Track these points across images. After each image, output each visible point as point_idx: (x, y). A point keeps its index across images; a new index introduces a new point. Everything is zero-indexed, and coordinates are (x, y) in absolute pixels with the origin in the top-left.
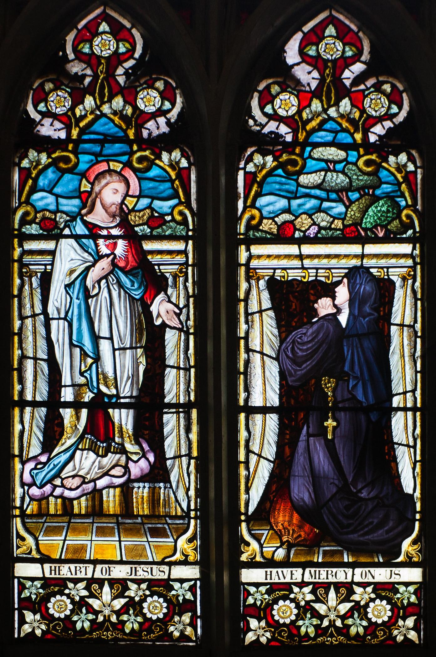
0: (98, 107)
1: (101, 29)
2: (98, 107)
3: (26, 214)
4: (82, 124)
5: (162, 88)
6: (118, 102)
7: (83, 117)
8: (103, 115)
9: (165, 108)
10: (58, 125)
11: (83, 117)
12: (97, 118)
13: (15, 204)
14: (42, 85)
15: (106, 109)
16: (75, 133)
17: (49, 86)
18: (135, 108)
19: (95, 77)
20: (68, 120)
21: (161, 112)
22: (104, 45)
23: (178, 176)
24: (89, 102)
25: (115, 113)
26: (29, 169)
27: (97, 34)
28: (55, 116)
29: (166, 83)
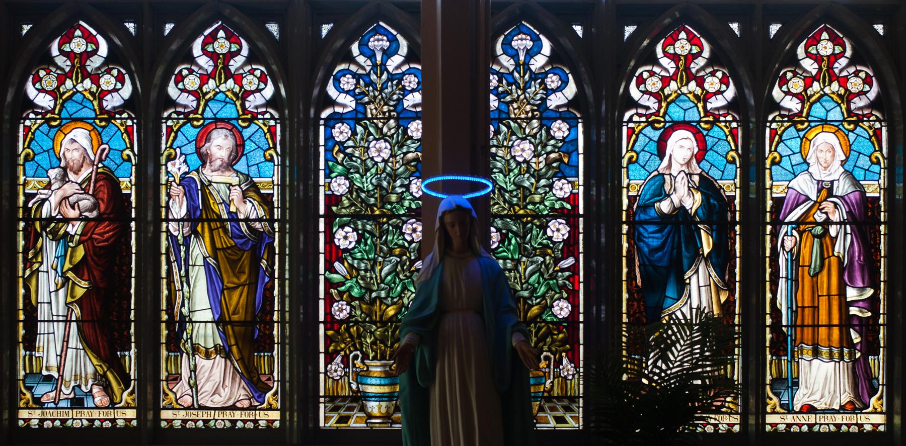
0: (218, 87)
1: (219, 36)
2: (218, 87)
3: (170, 155)
4: (207, 97)
5: (259, 75)
6: (231, 82)
7: (207, 93)
8: (221, 91)
9: (260, 87)
10: (192, 98)
11: (207, 93)
12: (217, 93)
13: (163, 147)
14: (181, 71)
15: (223, 88)
16: (202, 103)
17: (185, 72)
18: (241, 87)
19: (216, 67)
20: (198, 94)
21: (258, 90)
22: (222, 46)
23: (269, 130)
24: (212, 83)
25: (229, 90)
26: (171, 127)
27: (216, 39)
28: (190, 92)
29: (262, 72)
